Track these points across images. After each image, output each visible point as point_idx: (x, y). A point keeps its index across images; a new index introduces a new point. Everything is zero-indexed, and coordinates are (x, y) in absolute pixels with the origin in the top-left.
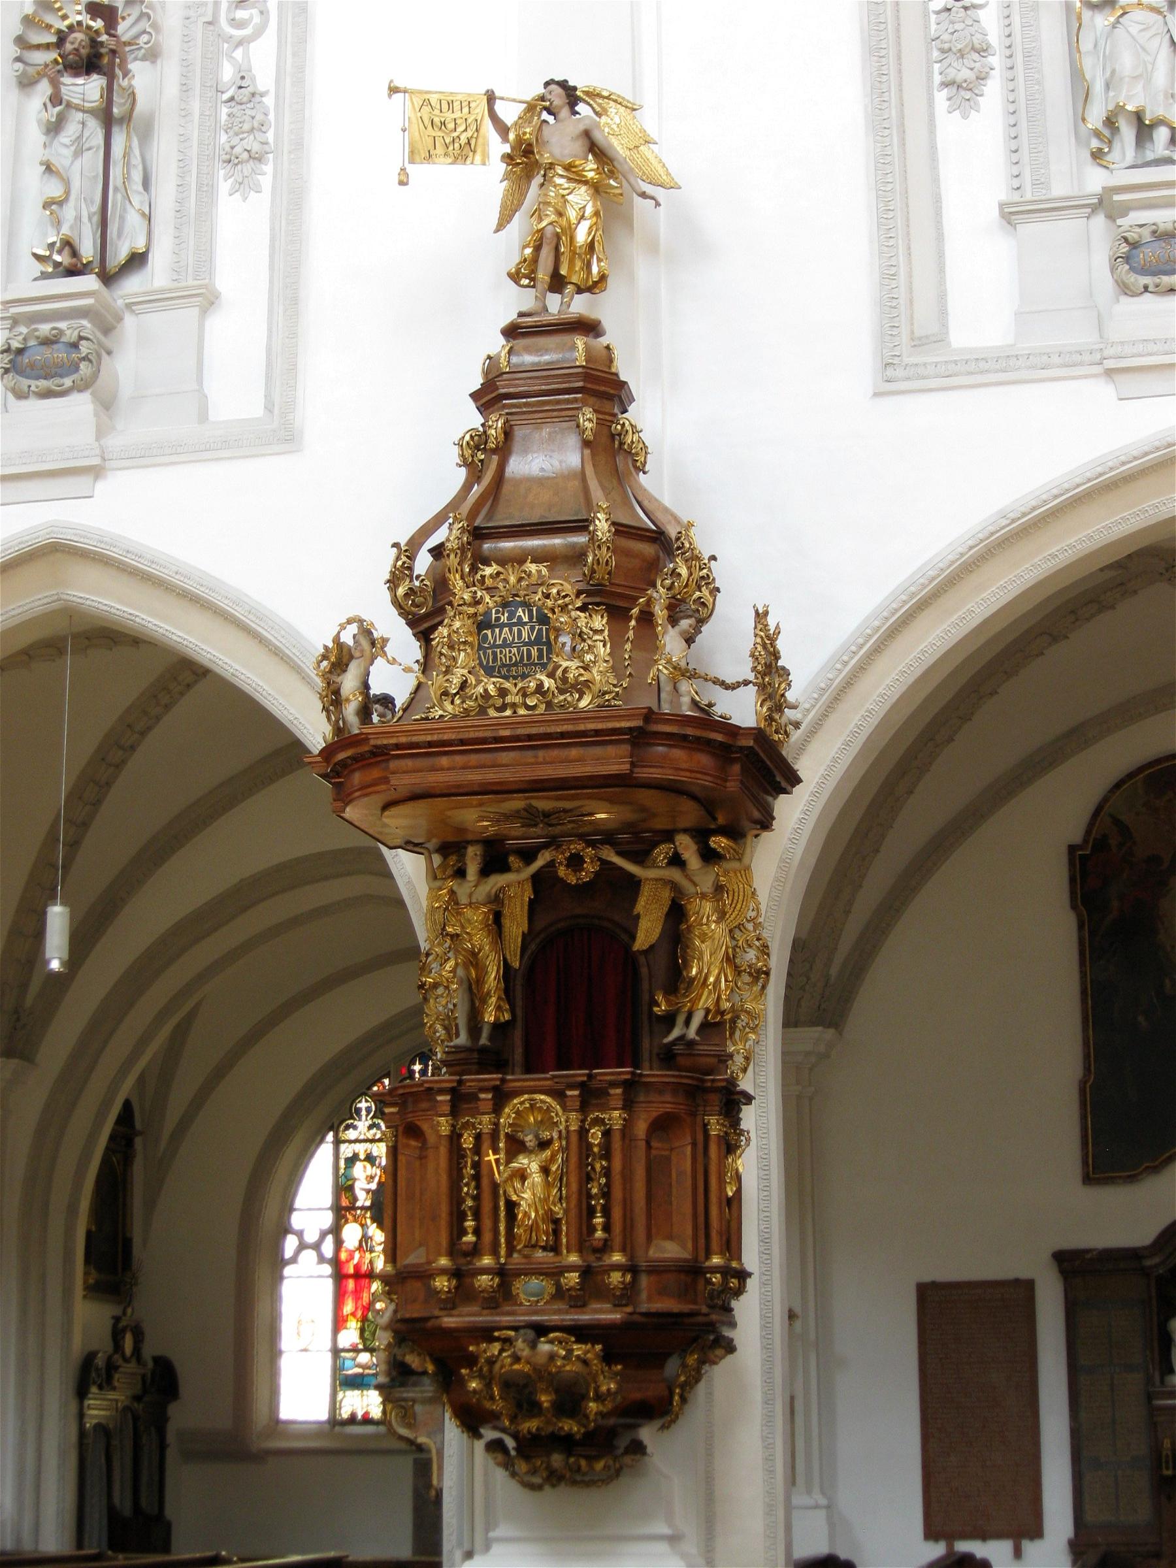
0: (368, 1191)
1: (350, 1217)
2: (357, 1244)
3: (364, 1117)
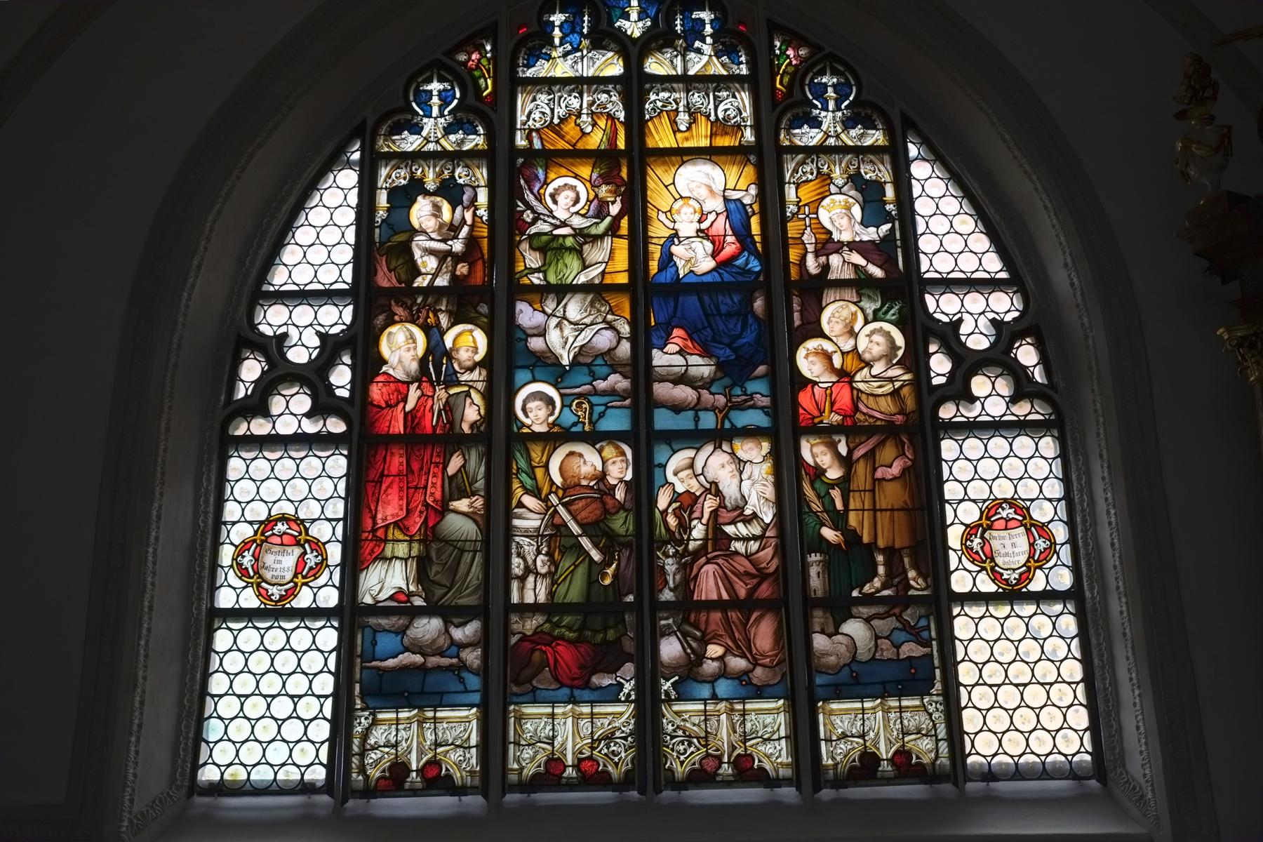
0: (442, 256)
2: (414, 366)
3: (435, 111)
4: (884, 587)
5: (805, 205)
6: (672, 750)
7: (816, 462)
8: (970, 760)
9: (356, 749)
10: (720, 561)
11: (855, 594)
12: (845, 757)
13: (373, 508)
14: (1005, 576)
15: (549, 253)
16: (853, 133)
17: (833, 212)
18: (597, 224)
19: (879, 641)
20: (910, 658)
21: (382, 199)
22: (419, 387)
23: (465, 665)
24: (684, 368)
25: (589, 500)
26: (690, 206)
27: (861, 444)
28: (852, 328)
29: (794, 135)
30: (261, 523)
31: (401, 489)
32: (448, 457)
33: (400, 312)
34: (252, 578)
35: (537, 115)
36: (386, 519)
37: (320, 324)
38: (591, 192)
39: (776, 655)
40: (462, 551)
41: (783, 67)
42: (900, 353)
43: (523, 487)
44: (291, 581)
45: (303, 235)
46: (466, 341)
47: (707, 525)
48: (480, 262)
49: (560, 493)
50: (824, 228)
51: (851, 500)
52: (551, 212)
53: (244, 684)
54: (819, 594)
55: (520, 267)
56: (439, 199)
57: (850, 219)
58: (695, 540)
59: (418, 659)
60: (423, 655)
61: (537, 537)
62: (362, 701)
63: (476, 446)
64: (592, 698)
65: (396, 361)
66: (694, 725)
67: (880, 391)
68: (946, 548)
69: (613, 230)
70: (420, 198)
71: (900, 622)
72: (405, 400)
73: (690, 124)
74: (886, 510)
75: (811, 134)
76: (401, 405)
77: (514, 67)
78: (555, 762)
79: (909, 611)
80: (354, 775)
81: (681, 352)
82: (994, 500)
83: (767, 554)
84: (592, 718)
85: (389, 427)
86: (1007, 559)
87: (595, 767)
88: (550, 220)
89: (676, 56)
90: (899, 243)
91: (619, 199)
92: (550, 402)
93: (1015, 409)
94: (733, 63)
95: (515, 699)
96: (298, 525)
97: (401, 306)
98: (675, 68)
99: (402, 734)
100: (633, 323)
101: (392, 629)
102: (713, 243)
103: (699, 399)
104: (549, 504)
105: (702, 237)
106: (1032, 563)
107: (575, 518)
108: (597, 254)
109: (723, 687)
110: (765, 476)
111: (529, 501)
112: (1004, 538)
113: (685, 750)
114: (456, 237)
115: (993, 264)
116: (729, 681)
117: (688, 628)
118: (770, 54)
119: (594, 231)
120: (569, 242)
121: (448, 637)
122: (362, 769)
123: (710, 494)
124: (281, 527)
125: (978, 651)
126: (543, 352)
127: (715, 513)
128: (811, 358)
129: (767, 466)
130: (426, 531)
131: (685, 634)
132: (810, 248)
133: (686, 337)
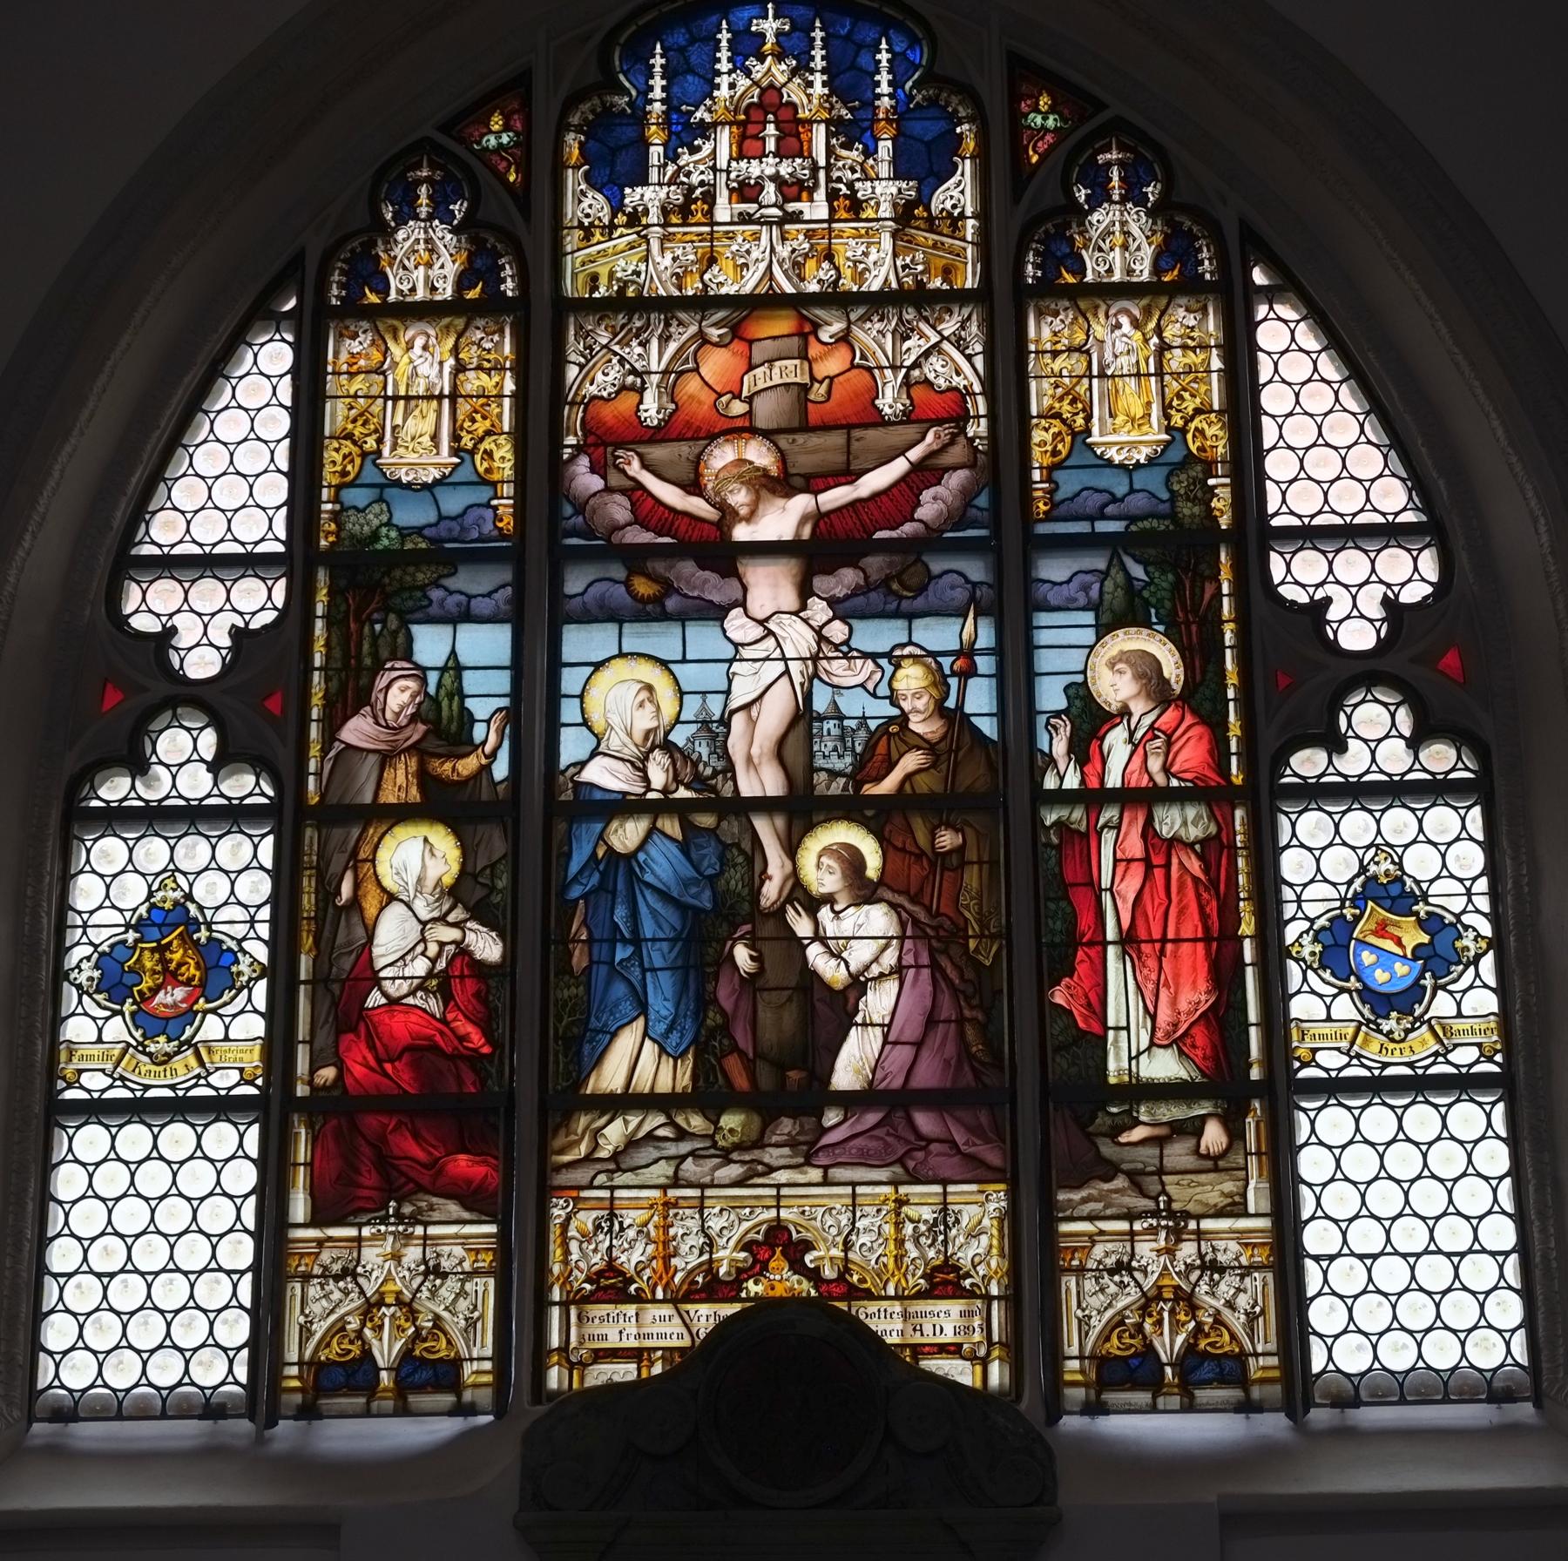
45: (208, 459)
115: (1393, 498)
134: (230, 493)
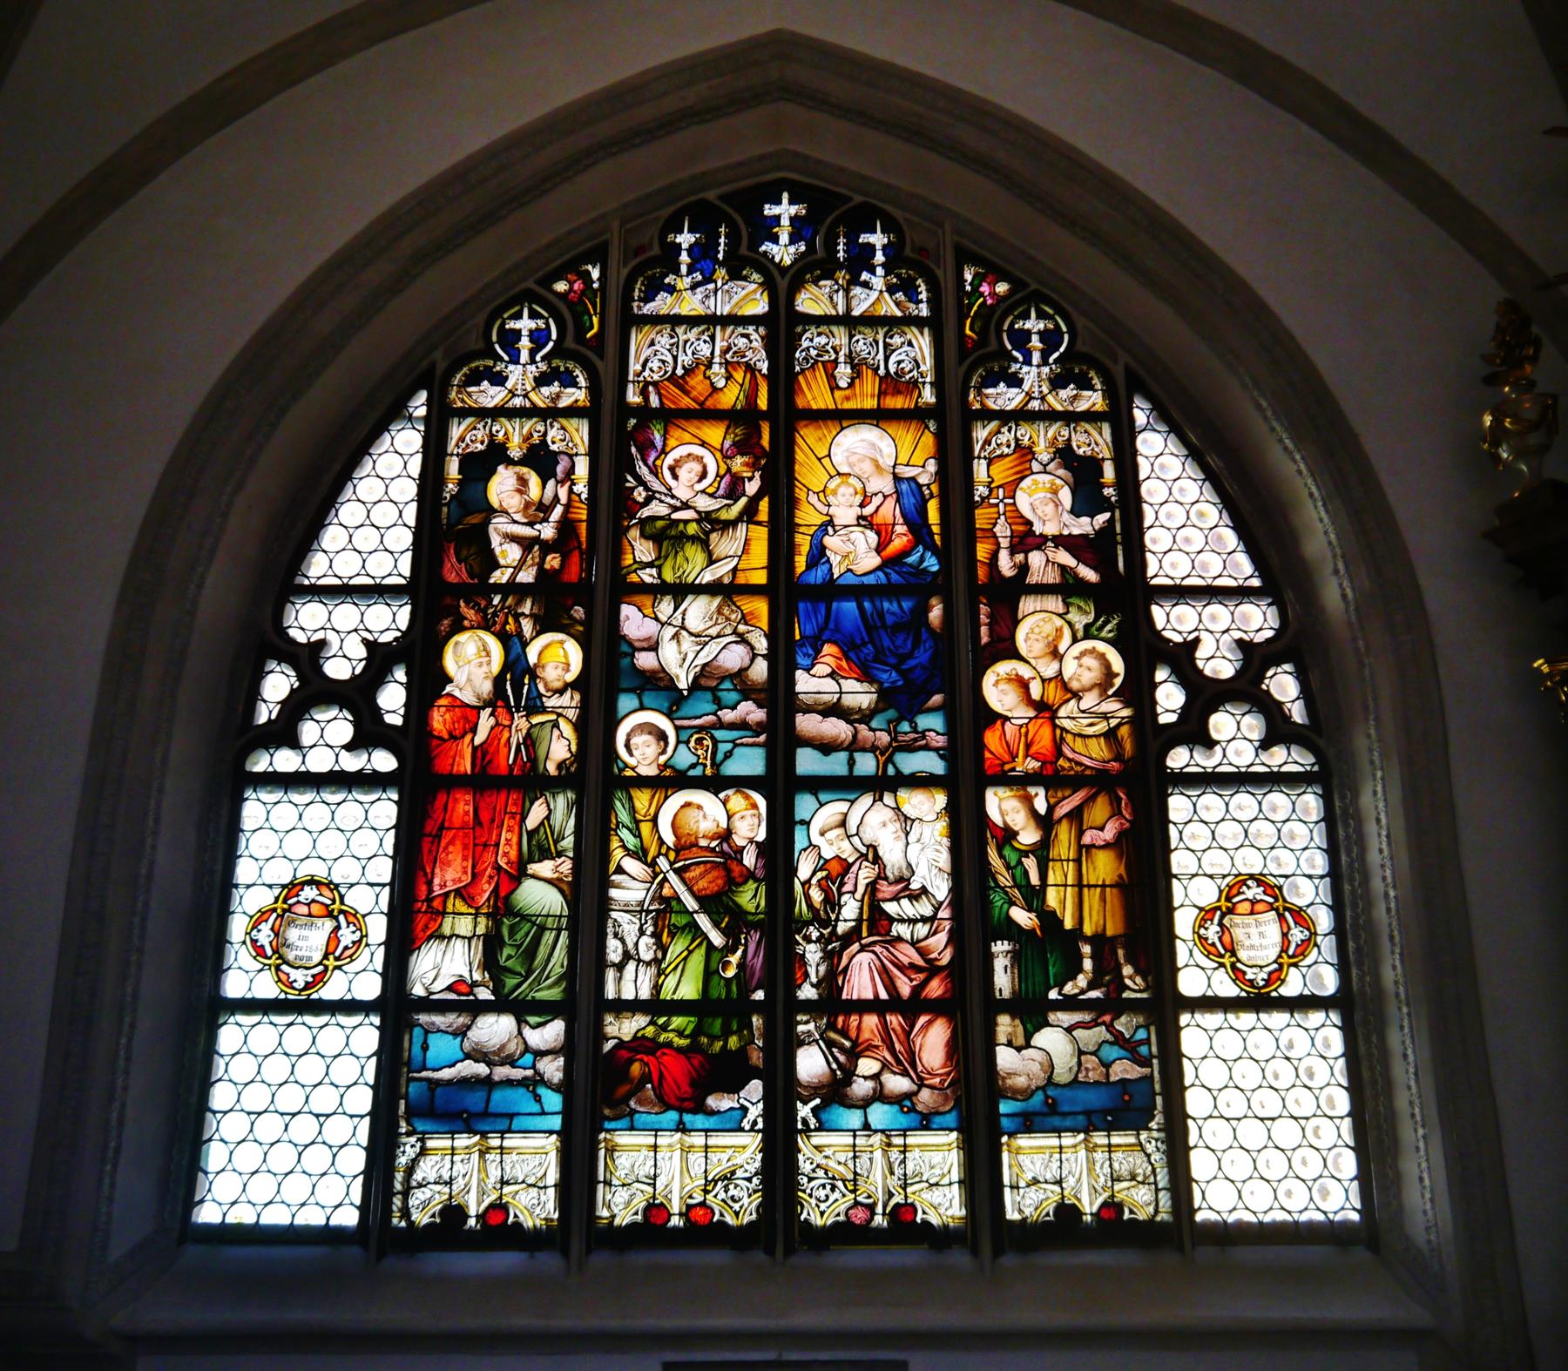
0: (526, 544)
1: (470, 614)
2: (487, 687)
3: (524, 356)
4: (1092, 986)
5: (998, 487)
6: (810, 1196)
7: (1005, 823)
8: (1199, 1217)
9: (398, 1187)
10: (878, 949)
11: (1053, 995)
12: (1036, 1209)
13: (428, 870)
14: (1249, 976)
15: (665, 544)
16: (1065, 394)
17: (1035, 497)
18: (729, 506)
19: (1083, 1058)
20: (1123, 1081)
21: (453, 468)
22: (492, 714)
23: (543, 1078)
24: (837, 696)
25: (709, 866)
26: (849, 485)
27: (1064, 798)
28: (1056, 648)
29: (987, 396)
30: (284, 887)
31: (465, 847)
32: (528, 804)
33: (470, 614)
34: (270, 958)
35: (655, 364)
36: (445, 886)
37: (367, 630)
38: (722, 464)
39: (948, 1074)
40: (542, 929)
41: (975, 308)
42: (1118, 682)
43: (624, 847)
44: (320, 963)
45: (349, 512)
46: (555, 655)
47: (862, 901)
48: (576, 553)
49: (672, 855)
50: (1022, 517)
51: (1051, 872)
52: (670, 489)
53: (256, 1098)
54: (1006, 994)
55: (628, 560)
56: (525, 470)
57: (1057, 506)
58: (845, 921)
59: (482, 1069)
60: (490, 1064)
61: (640, 912)
62: (408, 1123)
63: (564, 791)
64: (707, 1126)
65: (464, 679)
66: (840, 1163)
67: (1090, 731)
68: (1173, 937)
69: (749, 514)
70: (501, 468)
71: (1111, 1033)
72: (474, 731)
73: (853, 379)
74: (1096, 886)
75: (1008, 395)
76: (468, 738)
77: (627, 299)
78: (655, 1209)
79: (1123, 1019)
80: (395, 1221)
81: (832, 675)
82: (1236, 876)
83: (939, 941)
84: (706, 1152)
85: (453, 765)
86: (1252, 953)
87: (709, 1216)
88: (668, 500)
89: (837, 291)
90: (1119, 538)
91: (757, 475)
92: (662, 736)
93: (1264, 757)
94: (910, 301)
95: (607, 1125)
96: (332, 890)
97: (473, 608)
98: (835, 307)
99: (459, 1167)
100: (771, 636)
101: (450, 1030)
102: (878, 533)
103: (855, 736)
104: (657, 869)
105: (864, 526)
106: (1285, 960)
107: (690, 889)
108: (728, 545)
109: (880, 1115)
110: (939, 839)
111: (631, 865)
112: (1248, 925)
113: (827, 1197)
114: (545, 520)
115: (1243, 569)
116: (886, 1107)
117: (833, 1035)
118: (958, 292)
119: (724, 515)
120: (692, 529)
121: (521, 1041)
122: (405, 1212)
123: (867, 860)
124: (309, 893)
125: (1213, 1073)
126: (653, 672)
127: (872, 887)
128: (1002, 686)
129: (942, 825)
130: (496, 902)
131: (830, 1044)
132: (1004, 543)
133: (840, 655)
134: (366, 539)
